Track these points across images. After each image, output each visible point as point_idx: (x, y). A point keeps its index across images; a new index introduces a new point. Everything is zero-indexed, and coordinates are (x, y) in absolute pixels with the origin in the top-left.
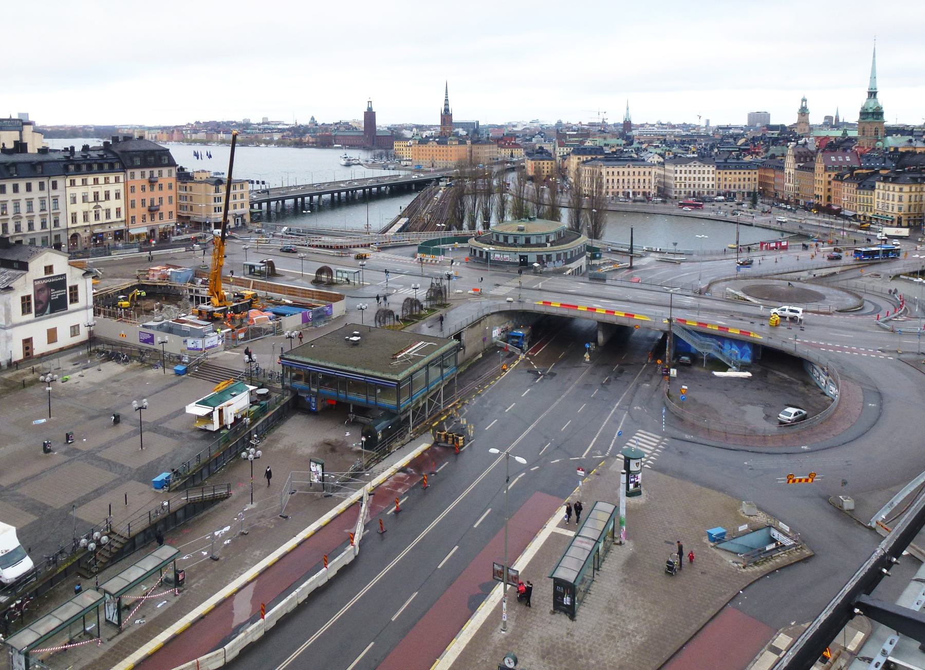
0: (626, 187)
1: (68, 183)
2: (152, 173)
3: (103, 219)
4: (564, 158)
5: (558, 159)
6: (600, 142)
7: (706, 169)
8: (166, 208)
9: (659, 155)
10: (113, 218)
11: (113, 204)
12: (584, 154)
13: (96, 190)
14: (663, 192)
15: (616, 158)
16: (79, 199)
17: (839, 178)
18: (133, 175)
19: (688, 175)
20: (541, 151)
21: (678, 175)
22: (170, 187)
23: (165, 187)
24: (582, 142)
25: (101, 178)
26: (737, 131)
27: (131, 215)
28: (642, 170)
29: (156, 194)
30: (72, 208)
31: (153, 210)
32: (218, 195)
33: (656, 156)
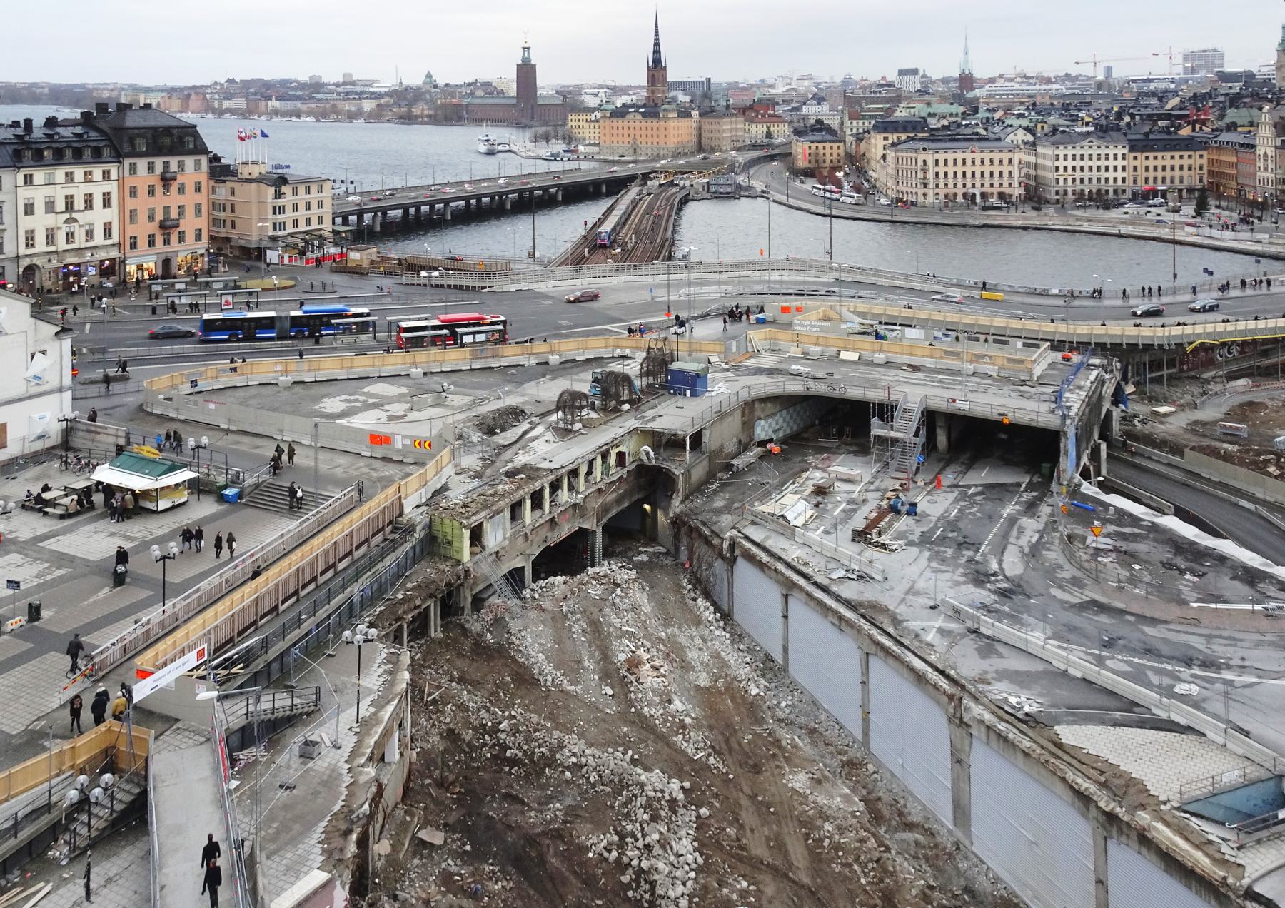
0: (969, 185)
1: (21, 180)
2: (166, 165)
3: (80, 241)
4: (859, 138)
5: (849, 139)
6: (919, 110)
7: (1111, 152)
8: (190, 224)
9: (1027, 129)
10: (99, 239)
11: (99, 216)
12: (896, 130)
13: (69, 192)
14: (1035, 196)
15: (951, 135)
16: (39, 207)
18: (133, 169)
19: (1078, 163)
20: (820, 126)
21: (1061, 163)
22: (198, 189)
23: (190, 188)
24: (889, 111)
25: (79, 172)
26: (1163, 86)
27: (129, 233)
28: (996, 156)
29: (174, 200)
30: (26, 223)
31: (167, 227)
32: (280, 202)
33: (1021, 132)
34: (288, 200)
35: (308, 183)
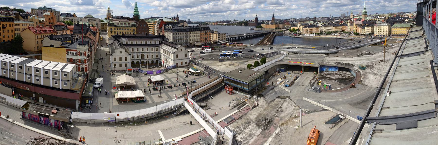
11: (198, 38)
17: (358, 26)
29: (206, 36)
30: (190, 38)
34: (220, 36)
35: (223, 34)
